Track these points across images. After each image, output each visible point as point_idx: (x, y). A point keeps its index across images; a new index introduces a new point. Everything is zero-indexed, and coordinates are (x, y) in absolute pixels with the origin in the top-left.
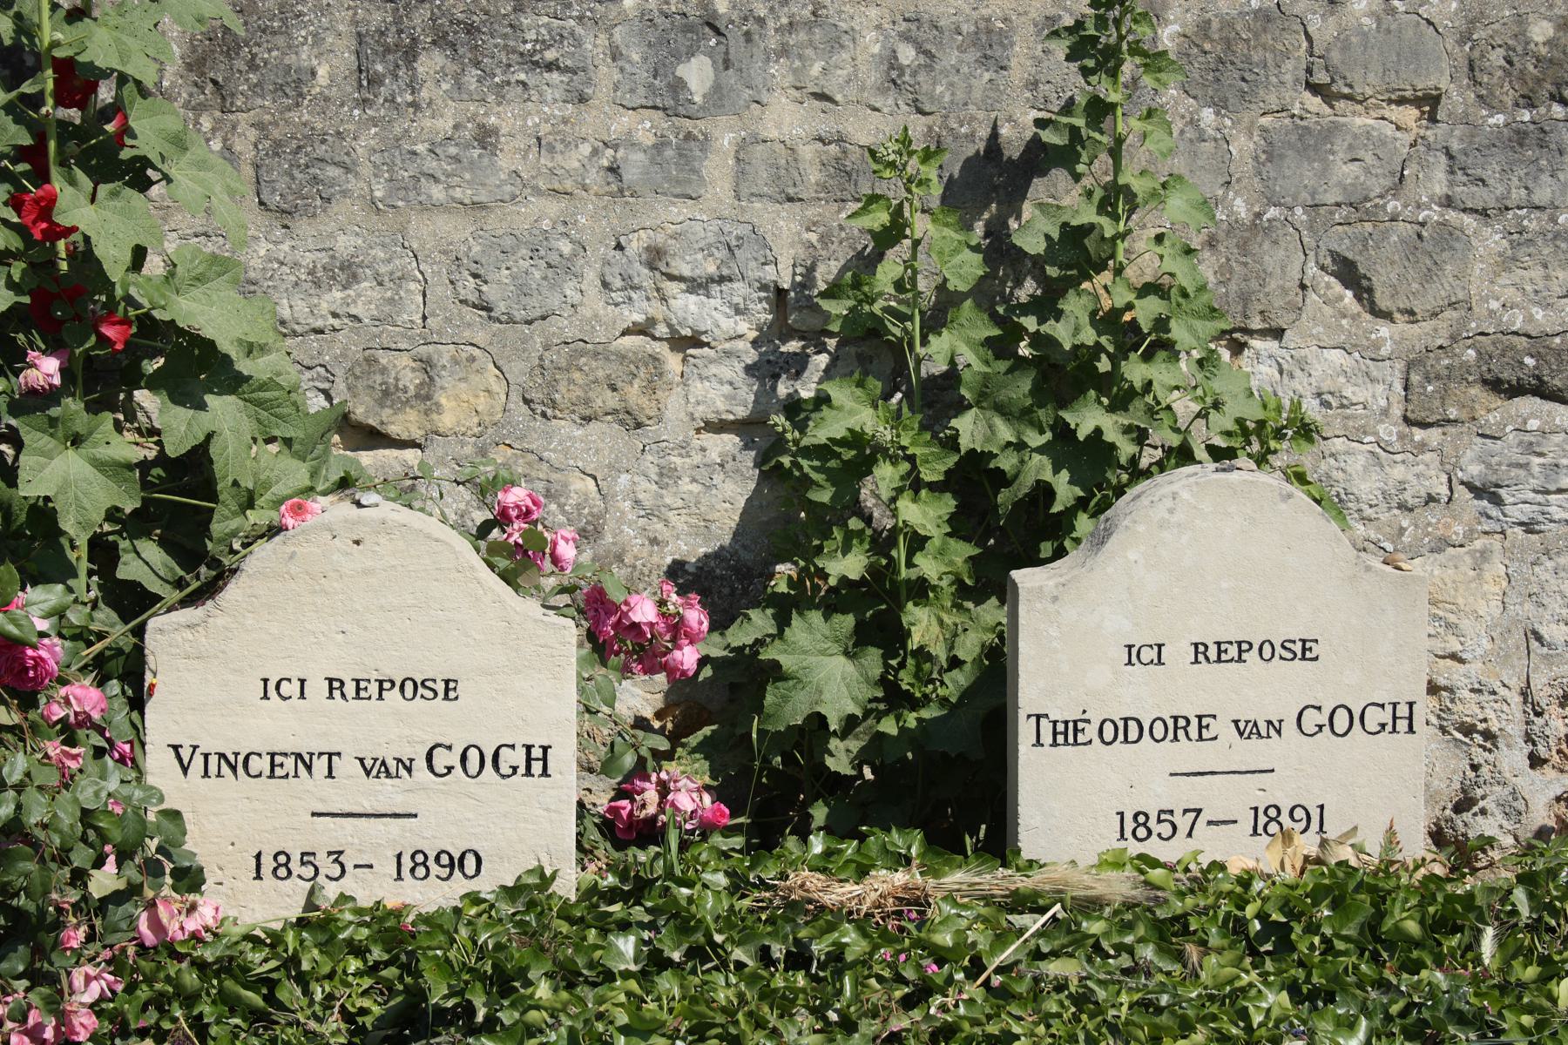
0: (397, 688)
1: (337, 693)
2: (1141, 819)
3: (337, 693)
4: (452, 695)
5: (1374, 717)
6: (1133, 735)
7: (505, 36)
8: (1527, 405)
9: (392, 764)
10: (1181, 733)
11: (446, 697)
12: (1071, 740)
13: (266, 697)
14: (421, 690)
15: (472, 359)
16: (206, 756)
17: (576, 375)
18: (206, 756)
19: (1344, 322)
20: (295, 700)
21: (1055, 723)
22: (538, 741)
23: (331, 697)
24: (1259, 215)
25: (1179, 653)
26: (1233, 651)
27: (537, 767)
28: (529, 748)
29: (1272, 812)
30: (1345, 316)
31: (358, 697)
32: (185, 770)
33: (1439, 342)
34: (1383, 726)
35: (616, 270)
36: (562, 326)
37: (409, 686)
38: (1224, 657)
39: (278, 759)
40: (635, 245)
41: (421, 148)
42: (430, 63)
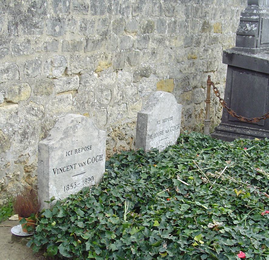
4: (91, 148)
7: (31, 22)
11: (90, 149)
13: (67, 156)
14: (87, 149)
16: (58, 170)
17: (41, 87)
18: (58, 170)
24: (121, 51)
32: (55, 173)
35: (46, 66)
36: (39, 77)
40: (49, 61)
41: (19, 44)
42: (20, 27)
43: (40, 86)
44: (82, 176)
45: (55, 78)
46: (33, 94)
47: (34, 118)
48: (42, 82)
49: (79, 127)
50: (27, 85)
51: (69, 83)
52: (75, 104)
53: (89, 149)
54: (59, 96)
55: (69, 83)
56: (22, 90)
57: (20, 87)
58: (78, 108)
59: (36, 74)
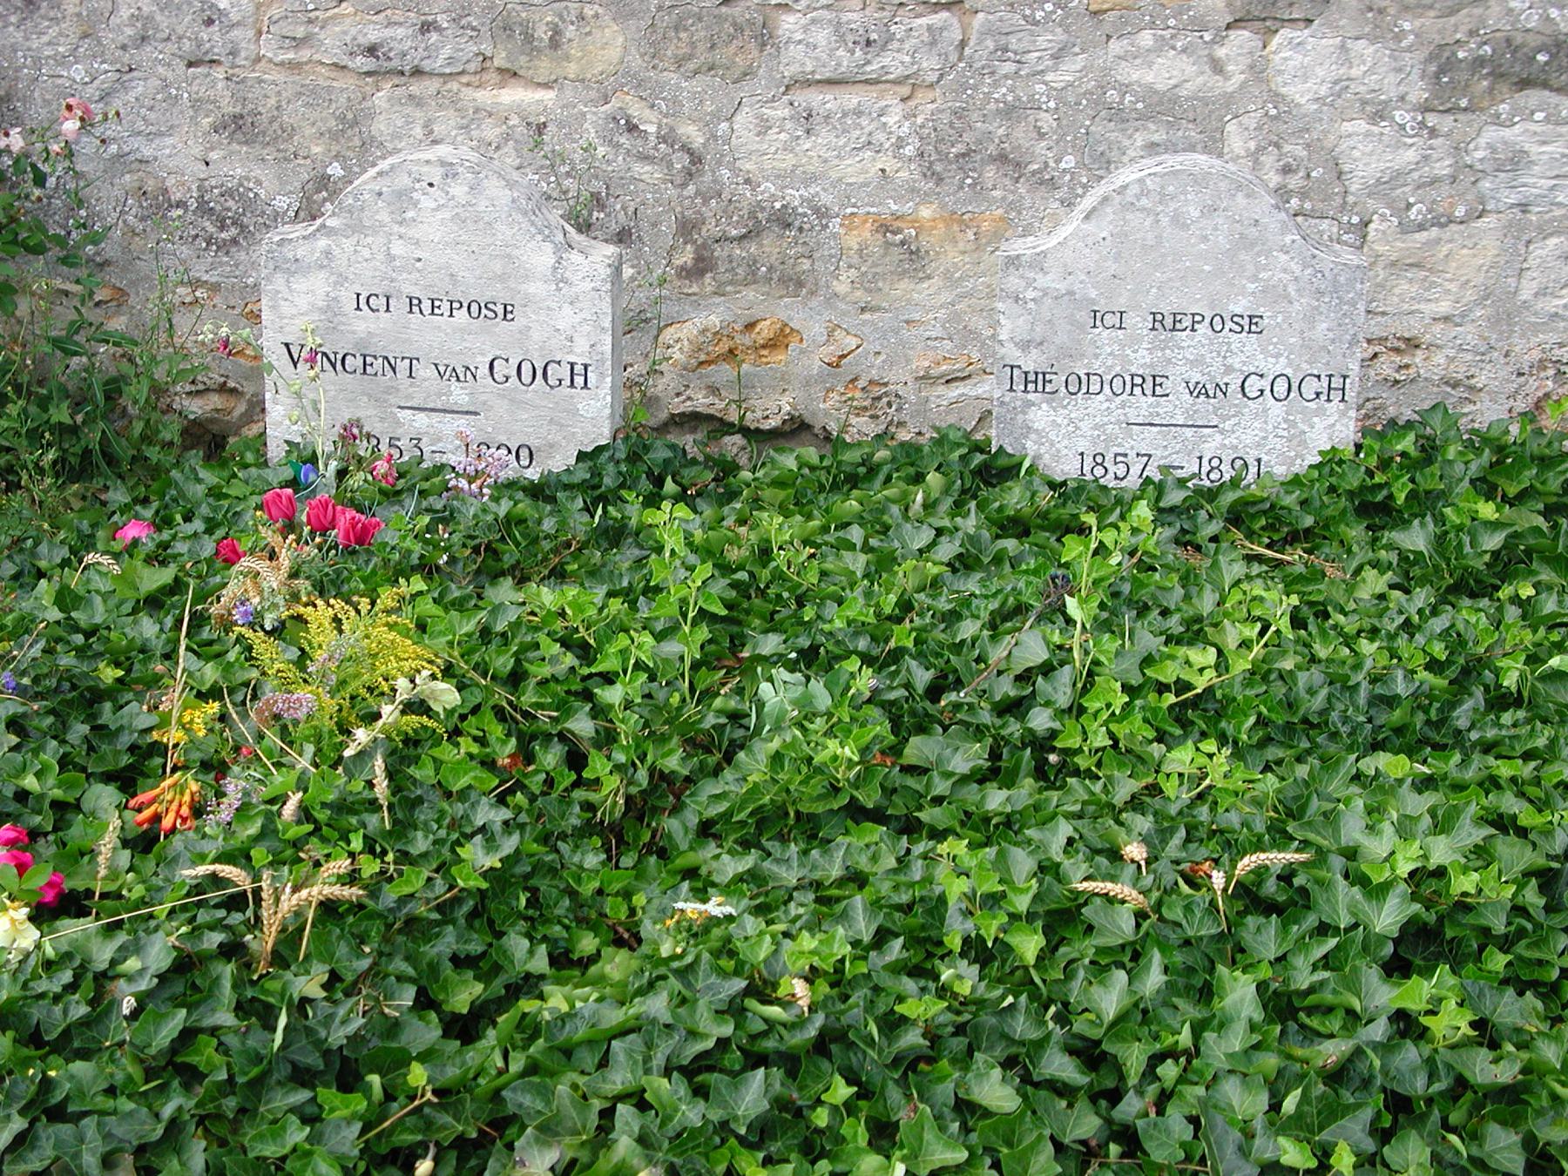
0: (465, 309)
1: (415, 309)
2: (1099, 459)
3: (415, 309)
4: (509, 316)
5: (1310, 387)
6: (1095, 388)
10: (1137, 390)
12: (1040, 388)
13: (358, 308)
14: (484, 311)
19: (1370, 15)
20: (382, 314)
21: (1026, 373)
22: (580, 361)
23: (411, 311)
25: (1138, 322)
26: (1187, 322)
27: (579, 380)
28: (572, 365)
29: (1215, 463)
30: (1371, 9)
31: (433, 313)
33: (1458, 36)
34: (1318, 394)
37: (474, 307)
38: (1178, 326)
44: (461, 422)
46: (636, 62)
49: (426, 203)
50: (596, 16)
52: (909, 151)
53: (501, 315)
56: (570, 31)
57: (561, 17)
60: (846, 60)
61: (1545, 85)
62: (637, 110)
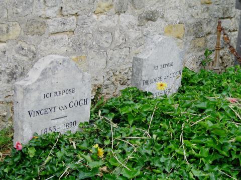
8: (150, 22)
9: (64, 107)
15: (16, 24)
36: (30, 17)
39: (46, 110)
43: (31, 25)
44: (63, 120)
45: (48, 18)
47: (25, 58)
48: (33, 21)
49: (59, 68)
50: (16, 24)
51: (64, 24)
52: (71, 45)
54: (53, 37)
55: (64, 24)
56: (11, 28)
57: (9, 25)
58: (74, 49)
59: (27, 12)
60: (60, 28)
61: (151, 20)
62: (23, 45)
